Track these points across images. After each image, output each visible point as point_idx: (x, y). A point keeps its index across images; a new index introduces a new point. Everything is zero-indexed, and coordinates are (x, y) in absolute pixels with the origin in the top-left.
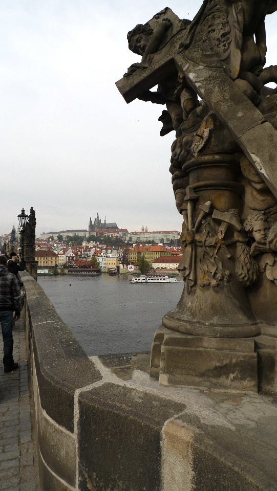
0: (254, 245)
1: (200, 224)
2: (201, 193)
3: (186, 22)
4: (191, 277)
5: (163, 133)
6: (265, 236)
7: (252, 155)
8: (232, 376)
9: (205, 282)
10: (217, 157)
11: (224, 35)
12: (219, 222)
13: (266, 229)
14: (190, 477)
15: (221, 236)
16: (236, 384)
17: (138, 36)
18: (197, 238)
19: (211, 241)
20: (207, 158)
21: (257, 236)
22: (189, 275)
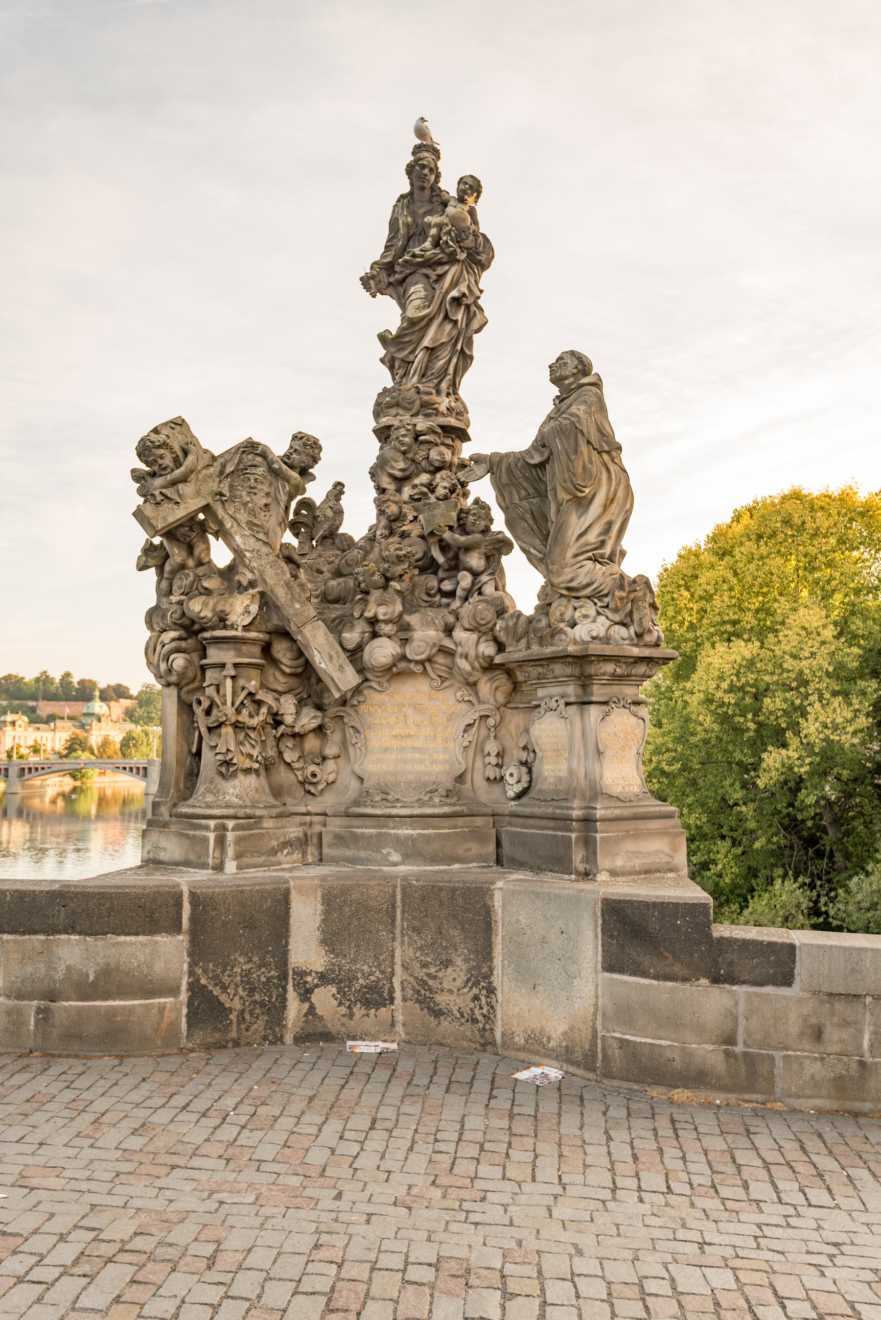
0: (283, 727)
1: (242, 703)
2: (241, 670)
3: (214, 458)
4: (235, 761)
5: (142, 568)
6: (295, 722)
7: (315, 652)
8: (285, 851)
9: (249, 766)
10: (261, 636)
11: (266, 505)
12: (259, 703)
13: (298, 713)
14: (319, 912)
15: (261, 718)
16: (289, 858)
17: (162, 451)
18: (240, 719)
19: (255, 722)
20: (253, 635)
21: (289, 719)
22: (231, 759)
